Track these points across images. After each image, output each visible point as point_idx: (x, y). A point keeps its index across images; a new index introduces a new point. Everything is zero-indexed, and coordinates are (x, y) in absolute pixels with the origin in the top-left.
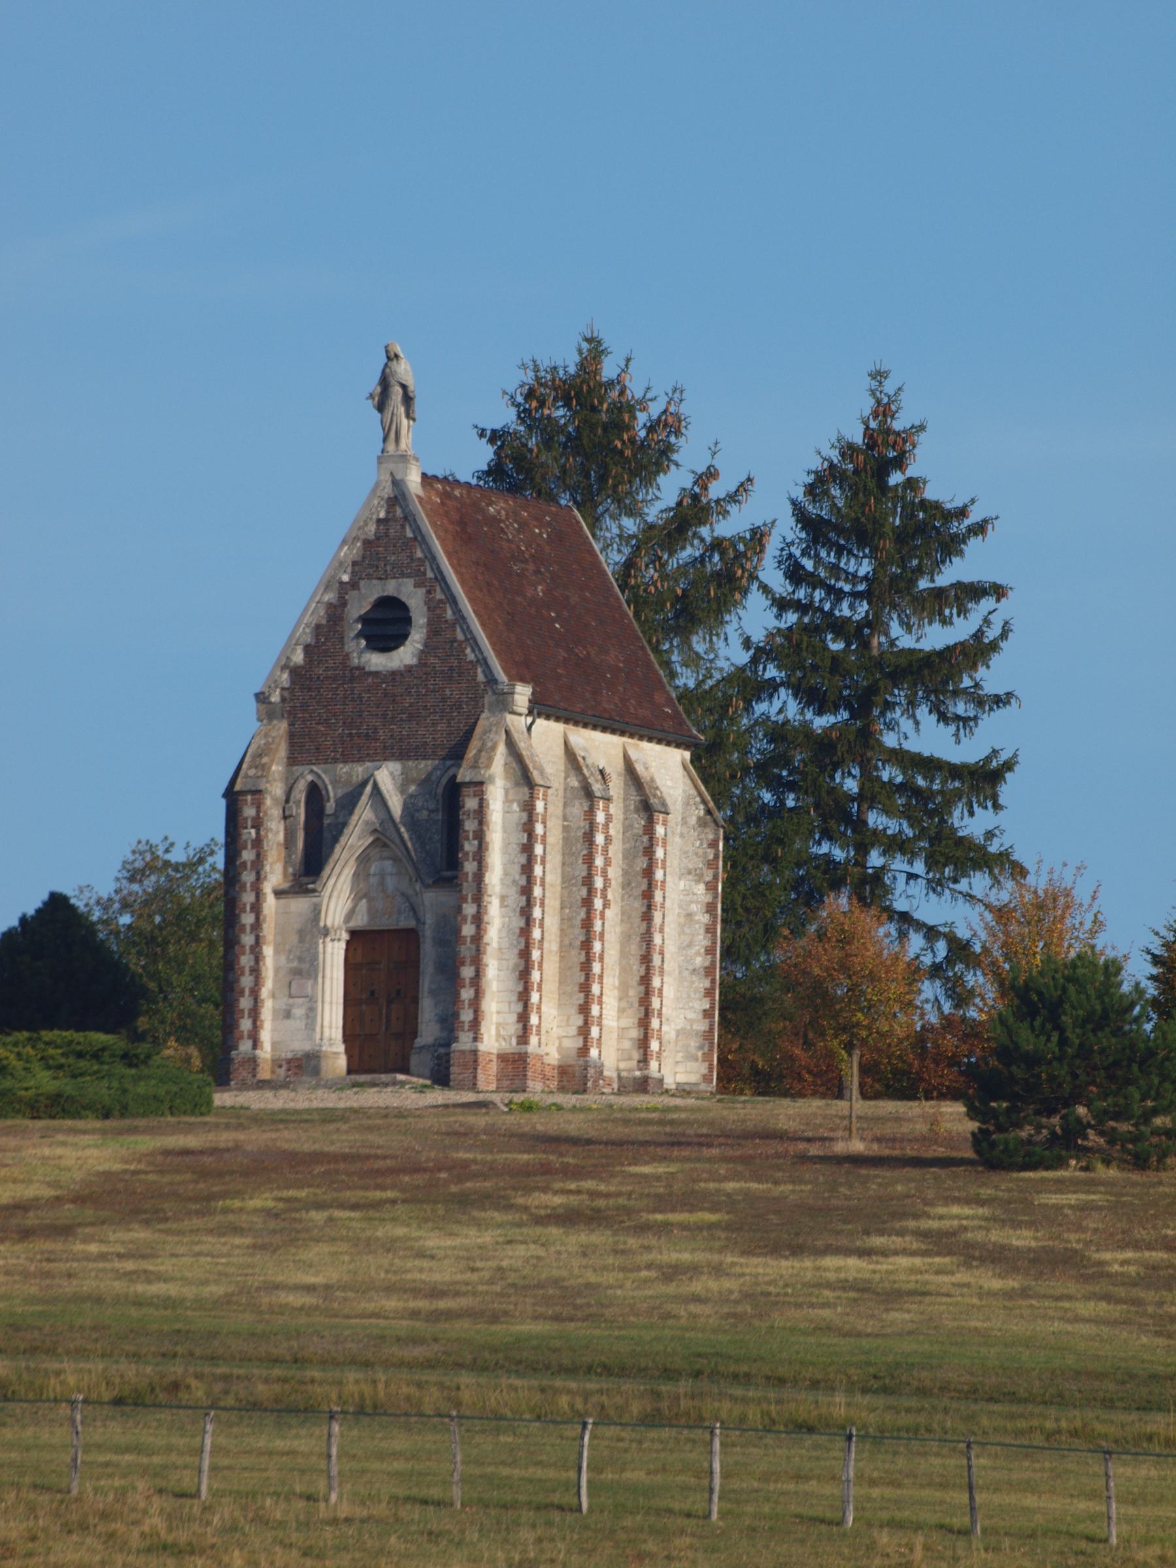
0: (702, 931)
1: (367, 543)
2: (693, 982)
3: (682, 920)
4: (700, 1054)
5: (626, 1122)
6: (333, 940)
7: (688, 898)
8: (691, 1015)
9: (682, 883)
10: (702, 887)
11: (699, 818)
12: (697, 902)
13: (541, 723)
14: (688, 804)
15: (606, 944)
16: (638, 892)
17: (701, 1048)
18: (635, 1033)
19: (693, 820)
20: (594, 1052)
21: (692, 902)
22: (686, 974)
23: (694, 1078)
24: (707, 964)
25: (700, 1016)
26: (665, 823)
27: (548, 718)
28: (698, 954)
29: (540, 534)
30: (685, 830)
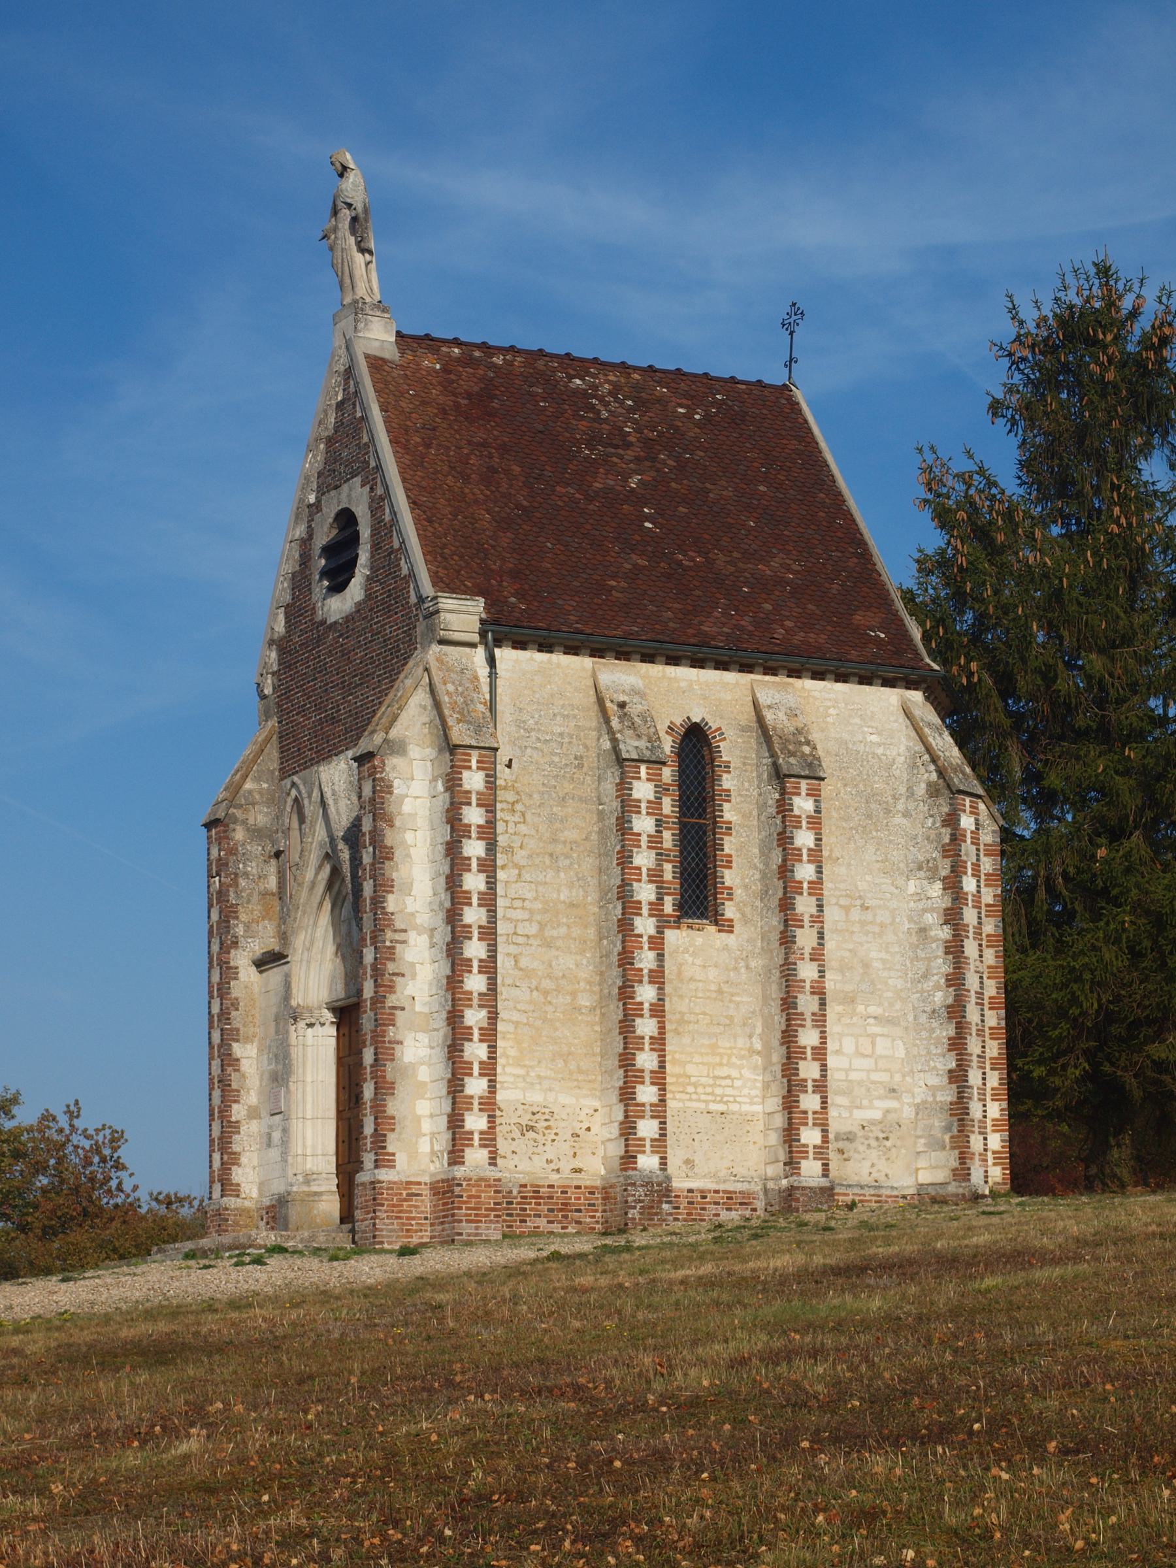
0: (940, 952)
1: (330, 441)
2: (932, 1030)
3: (914, 939)
4: (947, 1138)
5: (150, 1315)
6: (310, 1025)
7: (920, 905)
8: (934, 1081)
9: (912, 883)
10: (939, 885)
11: (929, 784)
12: (932, 910)
13: (506, 656)
14: (913, 766)
15: (668, 989)
16: (775, 903)
17: (948, 1128)
18: (779, 1121)
19: (921, 789)
20: (647, 1162)
21: (925, 911)
22: (923, 1018)
23: (940, 1176)
24: (950, 1001)
25: (945, 1080)
26: (814, 794)
27: (520, 645)
28: (937, 987)
29: (689, 416)
30: (911, 805)
